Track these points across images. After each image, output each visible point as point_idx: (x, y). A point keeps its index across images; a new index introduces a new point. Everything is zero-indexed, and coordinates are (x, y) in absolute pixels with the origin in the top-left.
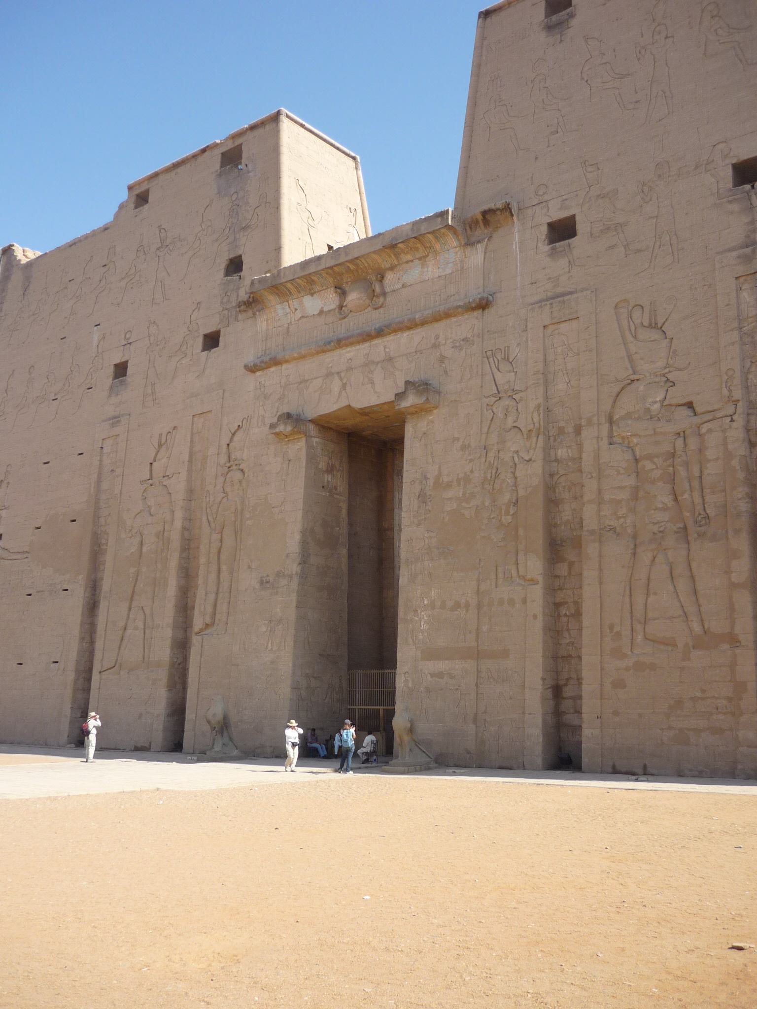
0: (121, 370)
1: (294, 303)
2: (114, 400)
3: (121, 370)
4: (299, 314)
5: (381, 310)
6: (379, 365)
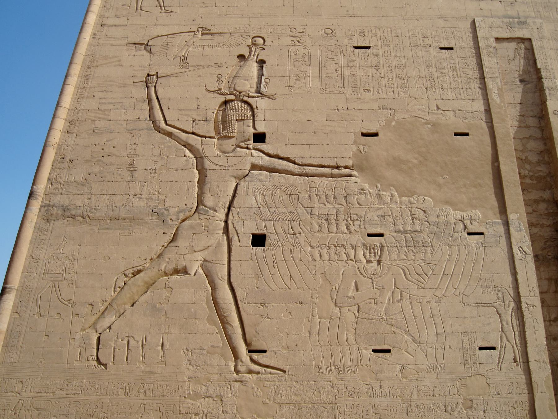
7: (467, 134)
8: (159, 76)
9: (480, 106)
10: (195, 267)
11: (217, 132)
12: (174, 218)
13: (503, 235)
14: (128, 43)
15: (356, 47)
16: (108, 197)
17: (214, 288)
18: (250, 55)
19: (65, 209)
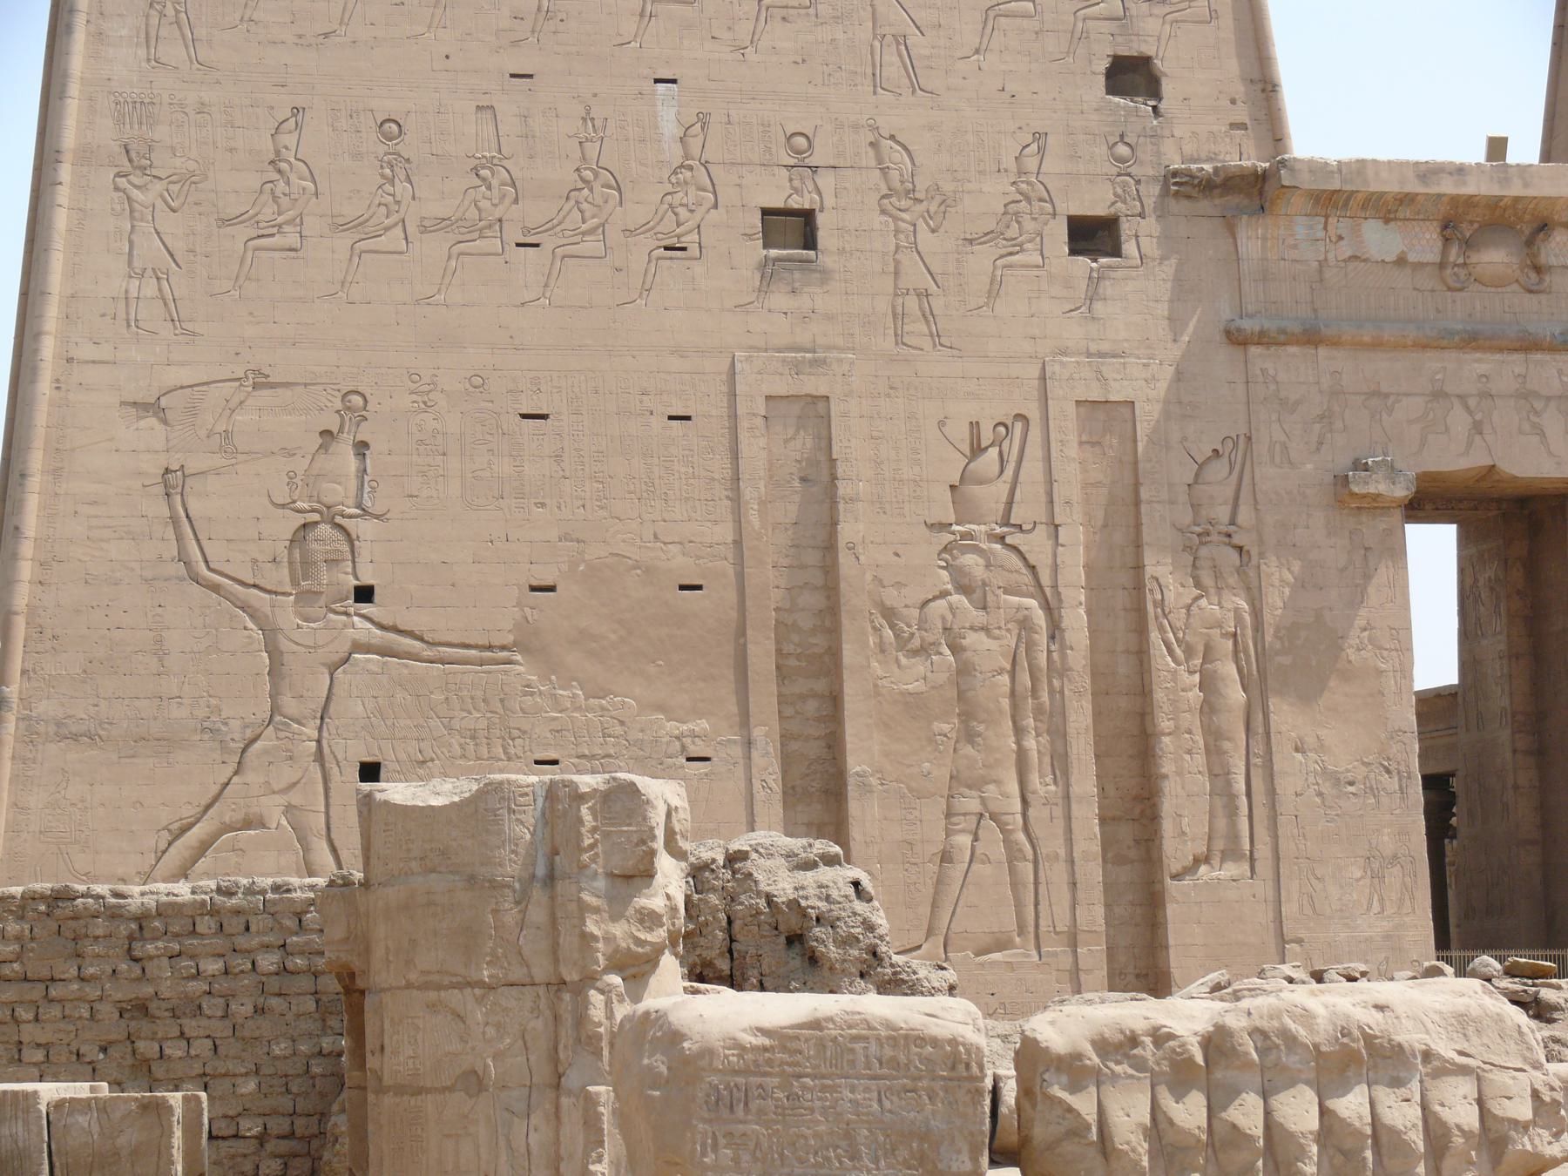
0: (793, 228)
1: (1339, 225)
2: (779, 299)
3: (793, 228)
4: (1346, 250)
5: (1543, 297)
6: (1553, 404)
7: (699, 587)
8: (187, 472)
9: (725, 532)
10: (276, 817)
11: (295, 582)
12: (237, 736)
13: (741, 762)
14: (123, 403)
15: (524, 416)
16: (126, 702)
17: (306, 849)
18: (341, 430)
19: (59, 724)
